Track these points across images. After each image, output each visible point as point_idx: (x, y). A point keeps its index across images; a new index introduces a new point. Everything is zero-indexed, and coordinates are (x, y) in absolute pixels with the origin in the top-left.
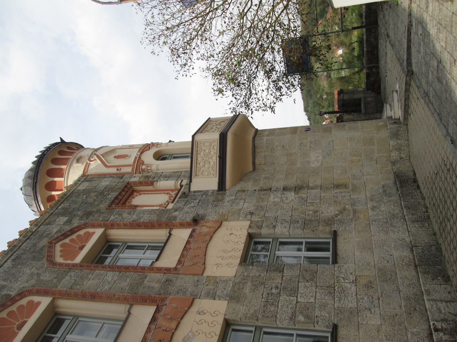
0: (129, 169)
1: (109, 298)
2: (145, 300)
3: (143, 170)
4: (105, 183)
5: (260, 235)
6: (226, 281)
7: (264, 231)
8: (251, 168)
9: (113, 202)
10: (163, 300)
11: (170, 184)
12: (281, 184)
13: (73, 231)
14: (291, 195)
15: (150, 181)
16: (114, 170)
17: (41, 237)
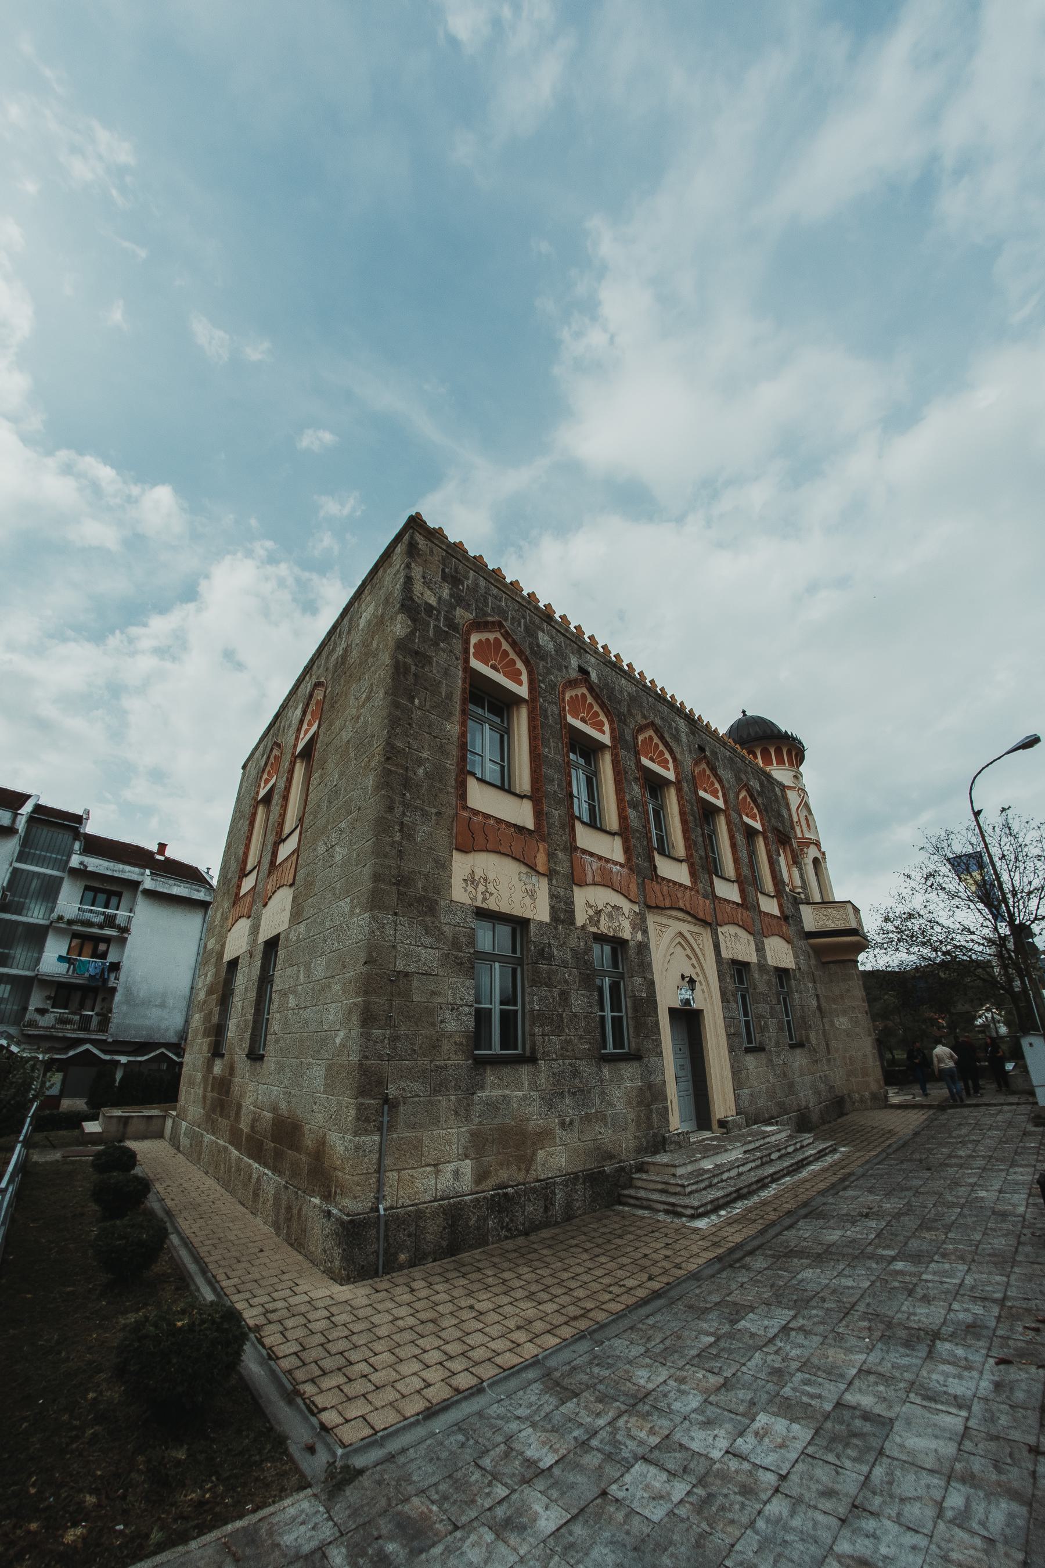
0: (799, 835)
1: (736, 861)
2: (742, 892)
3: (802, 850)
4: (785, 812)
5: (789, 979)
6: (765, 958)
7: (793, 983)
8: (824, 960)
9: (779, 831)
10: (747, 909)
11: (798, 882)
12: (819, 992)
13: (755, 801)
14: (815, 1003)
15: (796, 861)
16: (795, 819)
17: (746, 773)
